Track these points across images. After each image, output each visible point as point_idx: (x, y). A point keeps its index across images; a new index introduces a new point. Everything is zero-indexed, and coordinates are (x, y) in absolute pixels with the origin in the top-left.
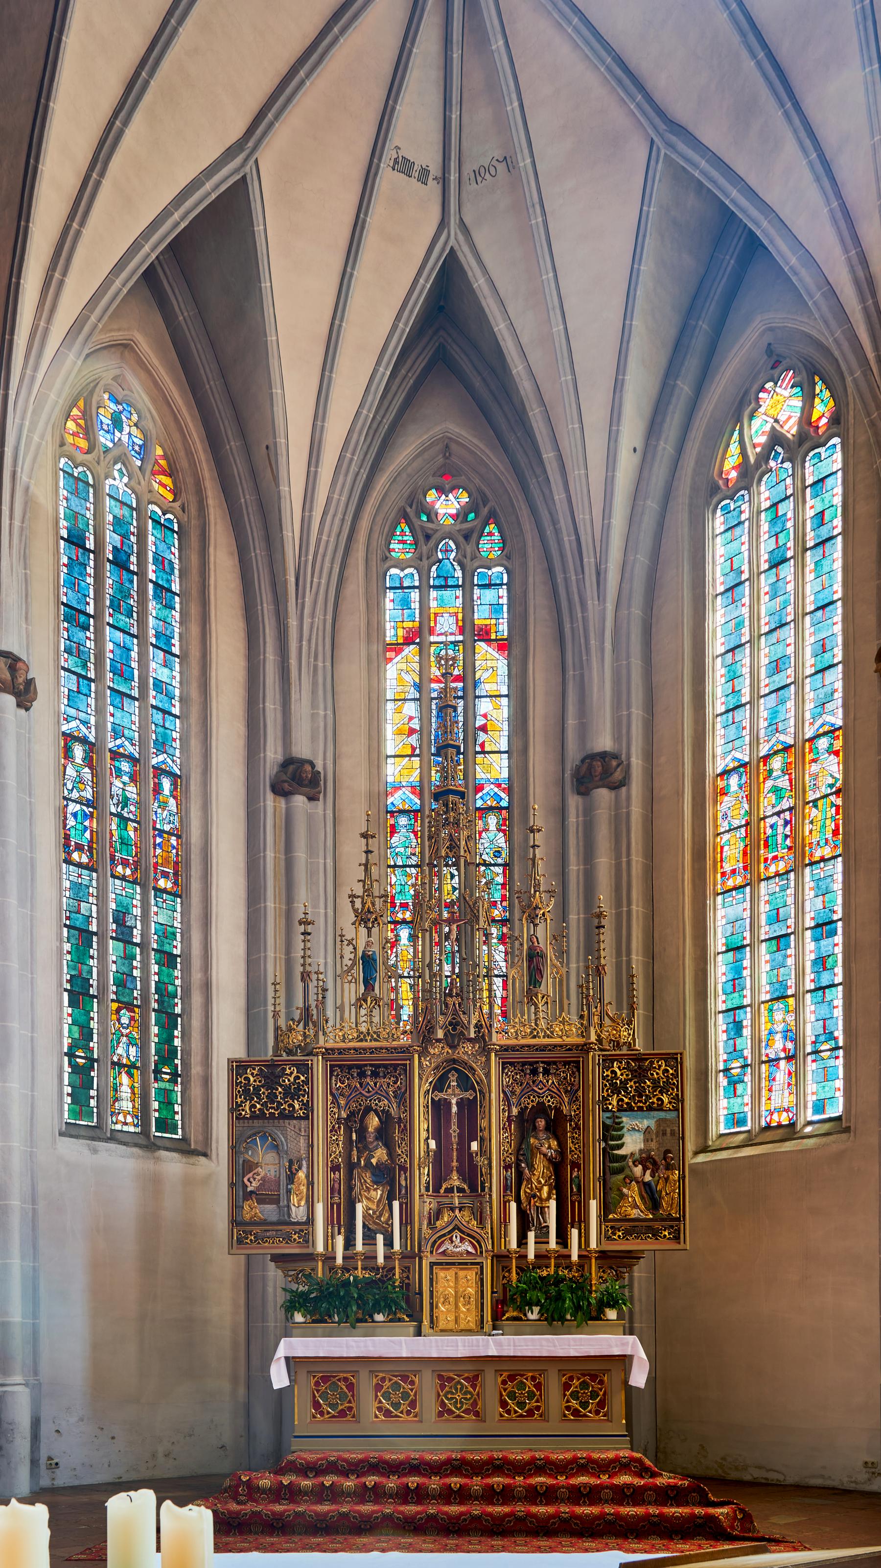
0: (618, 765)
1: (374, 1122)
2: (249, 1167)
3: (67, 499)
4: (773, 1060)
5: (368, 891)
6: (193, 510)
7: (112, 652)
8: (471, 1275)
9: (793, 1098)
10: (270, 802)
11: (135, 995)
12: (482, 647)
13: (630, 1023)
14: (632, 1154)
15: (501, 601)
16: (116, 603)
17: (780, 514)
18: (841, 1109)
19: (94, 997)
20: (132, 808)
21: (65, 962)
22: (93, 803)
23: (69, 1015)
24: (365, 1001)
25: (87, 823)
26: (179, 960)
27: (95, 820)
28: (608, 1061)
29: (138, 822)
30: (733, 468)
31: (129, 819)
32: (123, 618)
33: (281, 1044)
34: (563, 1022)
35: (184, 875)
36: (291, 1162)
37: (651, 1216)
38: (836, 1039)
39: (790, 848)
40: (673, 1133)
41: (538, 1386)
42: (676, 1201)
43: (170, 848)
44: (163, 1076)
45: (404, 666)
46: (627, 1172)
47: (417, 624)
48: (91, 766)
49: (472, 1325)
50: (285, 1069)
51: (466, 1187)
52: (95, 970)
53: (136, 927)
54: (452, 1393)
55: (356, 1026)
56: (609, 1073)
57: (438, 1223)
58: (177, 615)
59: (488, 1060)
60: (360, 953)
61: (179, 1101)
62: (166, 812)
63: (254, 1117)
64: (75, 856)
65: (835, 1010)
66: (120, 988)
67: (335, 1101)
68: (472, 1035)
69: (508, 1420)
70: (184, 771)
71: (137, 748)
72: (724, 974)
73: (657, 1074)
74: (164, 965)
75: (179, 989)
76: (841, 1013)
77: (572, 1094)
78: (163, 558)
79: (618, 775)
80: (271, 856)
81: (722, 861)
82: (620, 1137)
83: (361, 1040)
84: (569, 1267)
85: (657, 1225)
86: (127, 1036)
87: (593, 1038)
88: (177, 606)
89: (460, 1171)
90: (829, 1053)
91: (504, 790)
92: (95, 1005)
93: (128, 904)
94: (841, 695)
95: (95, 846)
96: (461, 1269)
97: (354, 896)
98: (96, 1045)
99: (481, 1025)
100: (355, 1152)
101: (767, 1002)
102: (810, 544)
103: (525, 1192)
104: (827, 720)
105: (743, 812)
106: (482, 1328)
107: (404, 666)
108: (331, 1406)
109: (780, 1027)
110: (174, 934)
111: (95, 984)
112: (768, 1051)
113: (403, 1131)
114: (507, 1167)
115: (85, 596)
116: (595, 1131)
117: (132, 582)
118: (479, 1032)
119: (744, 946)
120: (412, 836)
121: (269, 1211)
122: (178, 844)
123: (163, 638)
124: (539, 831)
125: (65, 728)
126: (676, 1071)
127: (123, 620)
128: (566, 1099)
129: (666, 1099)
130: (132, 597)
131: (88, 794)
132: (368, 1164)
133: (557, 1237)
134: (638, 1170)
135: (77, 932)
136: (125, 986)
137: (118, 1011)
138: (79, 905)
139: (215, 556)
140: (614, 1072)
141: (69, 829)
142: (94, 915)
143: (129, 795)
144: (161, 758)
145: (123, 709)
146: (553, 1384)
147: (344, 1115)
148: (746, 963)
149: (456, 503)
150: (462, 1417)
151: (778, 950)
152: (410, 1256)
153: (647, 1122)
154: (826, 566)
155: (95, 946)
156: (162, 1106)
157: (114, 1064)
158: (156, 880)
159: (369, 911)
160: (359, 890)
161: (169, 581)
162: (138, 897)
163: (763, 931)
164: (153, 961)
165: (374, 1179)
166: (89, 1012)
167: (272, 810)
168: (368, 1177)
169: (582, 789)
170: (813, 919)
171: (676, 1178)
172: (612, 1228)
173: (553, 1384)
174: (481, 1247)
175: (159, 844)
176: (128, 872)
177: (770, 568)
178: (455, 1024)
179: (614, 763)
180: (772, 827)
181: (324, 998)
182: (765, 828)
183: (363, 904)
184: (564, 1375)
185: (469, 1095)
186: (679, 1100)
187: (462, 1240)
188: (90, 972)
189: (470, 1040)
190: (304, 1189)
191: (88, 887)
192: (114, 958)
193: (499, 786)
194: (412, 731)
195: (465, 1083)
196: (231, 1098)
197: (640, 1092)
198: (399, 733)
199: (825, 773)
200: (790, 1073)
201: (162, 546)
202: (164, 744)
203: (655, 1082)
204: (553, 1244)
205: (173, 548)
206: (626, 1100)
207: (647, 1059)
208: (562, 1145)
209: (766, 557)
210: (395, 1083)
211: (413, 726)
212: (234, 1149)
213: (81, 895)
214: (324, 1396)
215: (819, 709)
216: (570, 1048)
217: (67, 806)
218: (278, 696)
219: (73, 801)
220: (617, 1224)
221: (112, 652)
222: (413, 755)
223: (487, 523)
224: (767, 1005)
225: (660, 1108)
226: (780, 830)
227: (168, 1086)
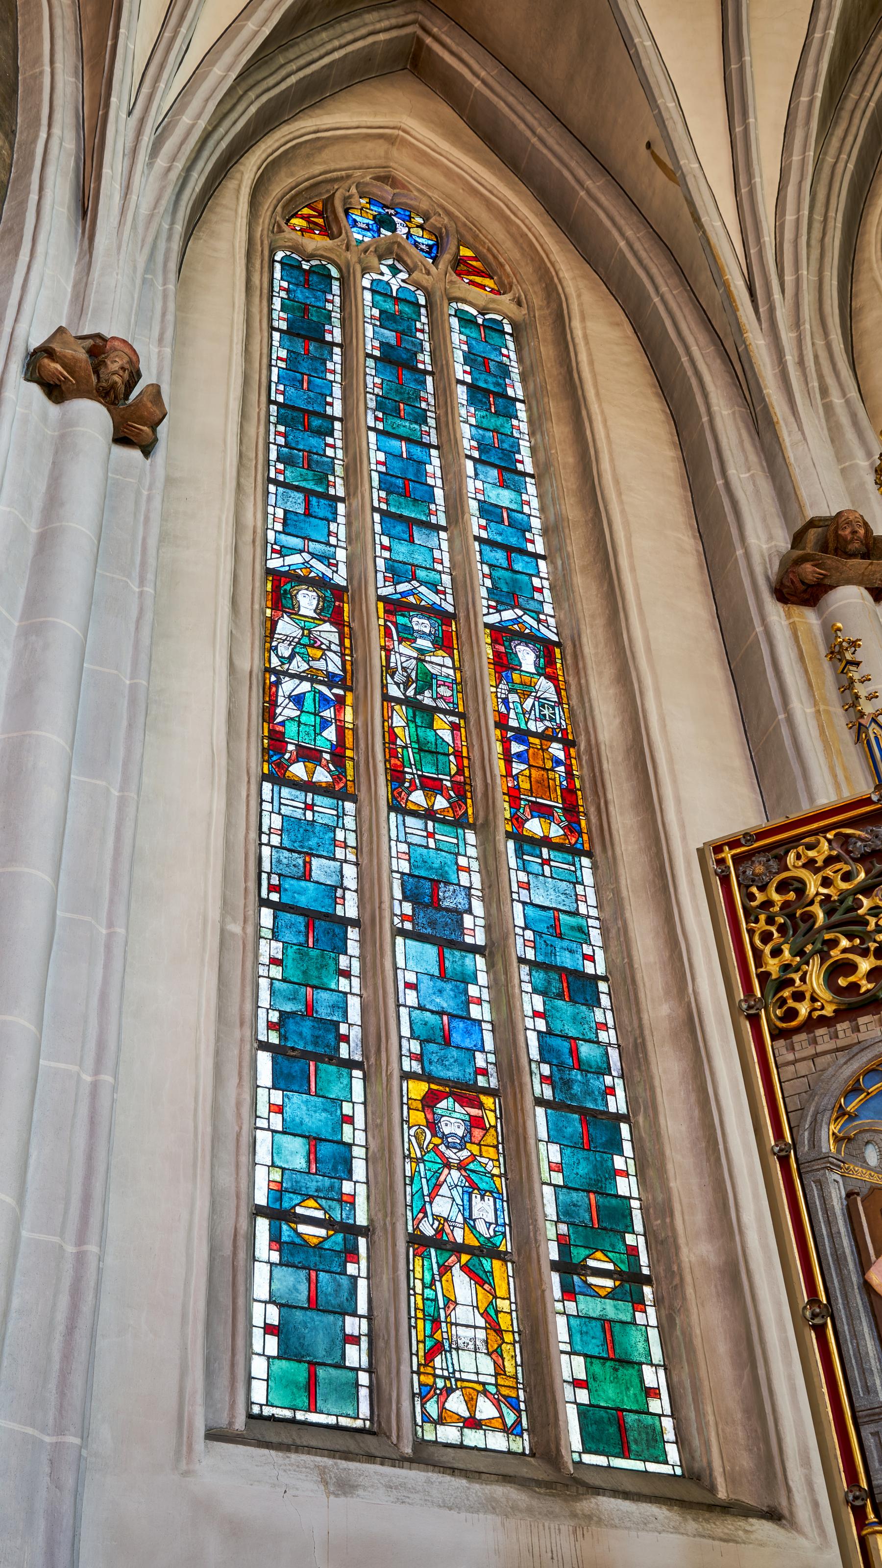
6: (537, 301)
16: (389, 404)
19: (350, 1064)
20: (444, 691)
21: (264, 983)
22: (344, 679)
25: (329, 713)
26: (603, 986)
27: (349, 711)
29: (462, 716)
31: (438, 710)
35: (592, 810)
43: (549, 765)
44: (592, 1280)
48: (337, 619)
52: (354, 1005)
53: (469, 911)
58: (524, 427)
61: (657, 1355)
62: (529, 703)
64: (298, 770)
66: (432, 1047)
70: (566, 632)
71: (450, 598)
74: (560, 996)
75: (614, 1054)
86: (461, 1166)
88: (523, 415)
92: (358, 1086)
93: (442, 865)
95: (349, 753)
98: (362, 1190)
111: (355, 1034)
122: (568, 756)
125: (275, 563)
131: (333, 664)
135: (301, 919)
136: (447, 1041)
138: (307, 865)
139: (584, 328)
141: (282, 724)
142: (350, 882)
143: (434, 670)
144: (508, 615)
145: (412, 541)
155: (353, 948)
156: (597, 1367)
157: (418, 1241)
158: (518, 821)
162: (472, 852)
164: (527, 987)
166: (338, 1102)
167: (788, 633)
175: (519, 755)
176: (441, 803)
191: (333, 829)
192: (411, 978)
202: (514, 595)
213: (313, 842)
217: (278, 683)
218: (753, 458)
219: (293, 676)
227: (610, 1309)
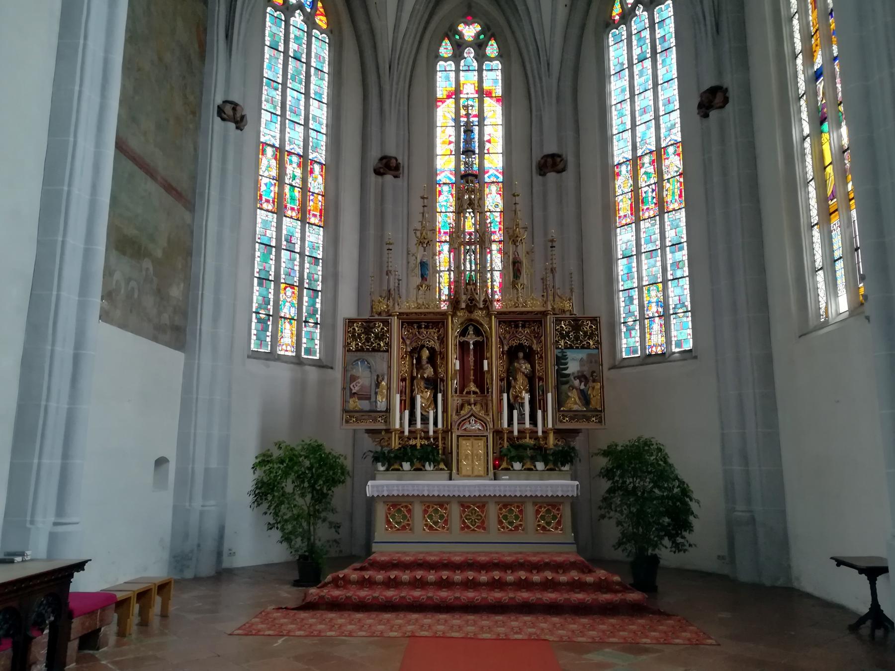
0: (561, 161)
1: (426, 353)
2: (353, 379)
3: (270, 27)
4: (651, 318)
5: (424, 227)
7: (290, 101)
8: (481, 443)
9: (664, 339)
10: (372, 178)
11: (295, 280)
12: (487, 100)
13: (570, 300)
14: (573, 373)
15: (498, 78)
17: (642, 36)
18: (691, 346)
23: (257, 291)
24: (422, 286)
28: (558, 321)
30: (617, 14)
32: (297, 84)
33: (374, 310)
34: (533, 299)
36: (378, 376)
37: (585, 409)
38: (686, 306)
39: (655, 204)
40: (596, 362)
41: (521, 511)
42: (599, 401)
45: (446, 109)
46: (571, 383)
47: (454, 89)
49: (482, 473)
50: (376, 324)
51: (478, 391)
54: (469, 515)
55: (417, 300)
56: (559, 327)
57: (462, 412)
59: (491, 319)
60: (419, 261)
63: (357, 350)
65: (685, 291)
67: (404, 342)
68: (482, 306)
69: (503, 533)
72: (622, 270)
73: (586, 328)
76: (689, 292)
77: (538, 337)
78: (320, 56)
79: (561, 166)
80: (372, 205)
81: (619, 210)
82: (566, 364)
83: (419, 308)
84: (537, 438)
85: (589, 414)
87: (550, 308)
89: (475, 382)
90: (683, 314)
91: (500, 173)
94: (679, 125)
96: (476, 439)
97: (416, 230)
99: (487, 301)
100: (415, 370)
101: (647, 285)
102: (659, 51)
103: (512, 394)
104: (673, 138)
105: (629, 185)
106: (488, 474)
107: (446, 109)
108: (397, 523)
109: (654, 300)
110: (319, 247)
112: (648, 313)
113: (442, 359)
114: (502, 380)
115: (277, 74)
116: (551, 360)
117: (302, 67)
118: (485, 304)
119: (632, 256)
120: (450, 196)
121: (364, 405)
123: (318, 95)
124: (518, 195)
126: (597, 326)
127: (297, 86)
128: (535, 342)
129: (591, 343)
130: (302, 74)
132: (422, 378)
133: (530, 420)
134: (577, 382)
137: (285, 288)
140: (562, 327)
146: (530, 510)
147: (409, 350)
148: (634, 264)
149: (474, 30)
150: (476, 531)
151: (652, 258)
152: (447, 431)
153: (582, 354)
154: (668, 61)
159: (424, 238)
160: (419, 227)
161: (322, 67)
163: (643, 247)
165: (425, 385)
168: (422, 384)
169: (542, 173)
170: (670, 241)
171: (599, 387)
172: (563, 415)
173: (530, 510)
174: (486, 426)
177: (638, 62)
178: (472, 300)
179: (559, 159)
180: (645, 192)
181: (399, 284)
182: (642, 193)
183: (421, 234)
184: (536, 505)
185: (479, 339)
186: (599, 343)
187: (476, 422)
188: (270, 268)
189: (480, 309)
190: (385, 391)
193: (497, 171)
194: (450, 143)
195: (478, 332)
196: (345, 340)
197: (577, 338)
198: (444, 143)
199: (673, 165)
200: (661, 325)
201: (319, 50)
203: (585, 333)
204: (527, 425)
205: (325, 51)
206: (569, 343)
207: (580, 320)
208: (533, 367)
209: (636, 57)
210: (439, 331)
211: (452, 140)
212: (345, 370)
214: (393, 517)
215: (668, 133)
216: (537, 313)
220: (565, 414)
221: (290, 101)
222: (451, 154)
223: (490, 40)
224: (647, 287)
225: (588, 347)
226: (650, 194)
